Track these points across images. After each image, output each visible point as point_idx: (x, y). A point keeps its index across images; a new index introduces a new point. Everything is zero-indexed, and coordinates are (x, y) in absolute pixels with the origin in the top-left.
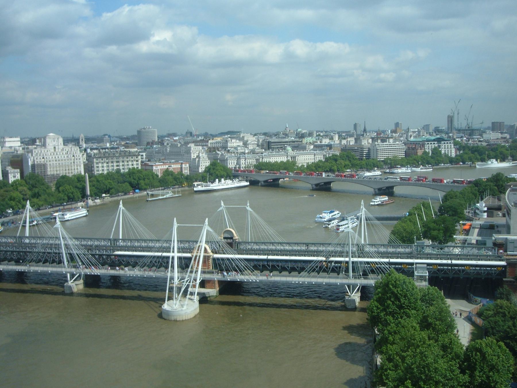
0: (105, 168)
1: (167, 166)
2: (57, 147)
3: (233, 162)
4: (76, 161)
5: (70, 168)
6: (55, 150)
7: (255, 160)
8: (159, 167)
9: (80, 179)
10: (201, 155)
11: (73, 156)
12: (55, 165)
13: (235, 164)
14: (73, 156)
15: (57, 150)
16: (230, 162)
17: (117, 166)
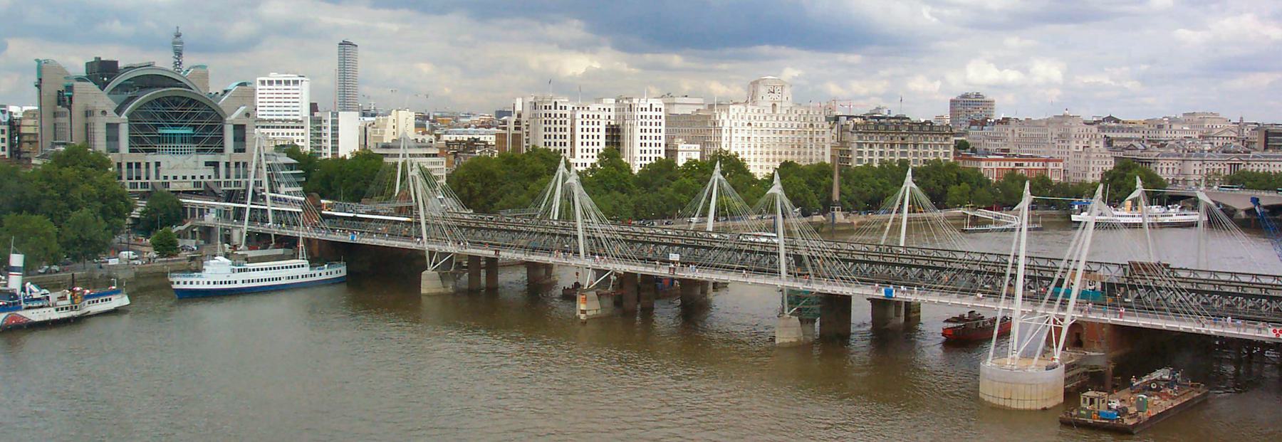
0: (876, 158)
1: (1013, 164)
2: (778, 105)
3: (1171, 166)
4: (815, 137)
5: (802, 150)
6: (774, 111)
7: (1228, 167)
8: (995, 165)
9: (822, 171)
10: (1093, 144)
11: (812, 125)
12: (772, 140)
13: (1176, 172)
14: (812, 125)
15: (778, 112)
16: (1165, 166)
17: (903, 153)
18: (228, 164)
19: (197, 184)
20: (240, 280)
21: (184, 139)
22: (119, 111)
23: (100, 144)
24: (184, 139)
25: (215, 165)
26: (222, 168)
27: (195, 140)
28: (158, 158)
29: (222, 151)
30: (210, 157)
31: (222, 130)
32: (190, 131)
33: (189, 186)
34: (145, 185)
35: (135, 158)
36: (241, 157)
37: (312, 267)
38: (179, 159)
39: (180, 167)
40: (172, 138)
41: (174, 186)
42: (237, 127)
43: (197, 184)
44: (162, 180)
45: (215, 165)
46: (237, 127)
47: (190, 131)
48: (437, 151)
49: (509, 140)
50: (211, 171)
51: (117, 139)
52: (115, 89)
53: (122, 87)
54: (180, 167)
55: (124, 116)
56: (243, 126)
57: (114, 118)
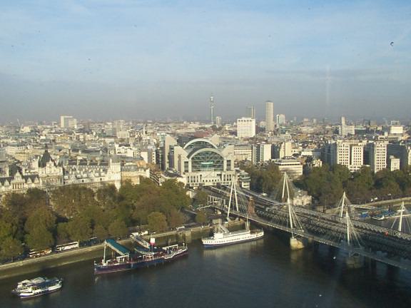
18: (225, 176)
19: (214, 183)
21: (210, 166)
22: (188, 157)
23: (183, 169)
24: (210, 166)
25: (220, 175)
26: (223, 177)
27: (214, 166)
28: (200, 173)
29: (222, 170)
31: (223, 162)
32: (212, 163)
34: (197, 184)
36: (229, 173)
37: (251, 233)
38: (208, 173)
40: (204, 166)
41: (206, 184)
42: (228, 161)
43: (214, 183)
44: (202, 182)
45: (220, 175)
46: (228, 161)
47: (212, 163)
48: (299, 163)
49: (326, 156)
50: (219, 178)
51: (188, 166)
53: (190, 146)
55: (190, 159)
56: (230, 161)
57: (187, 160)
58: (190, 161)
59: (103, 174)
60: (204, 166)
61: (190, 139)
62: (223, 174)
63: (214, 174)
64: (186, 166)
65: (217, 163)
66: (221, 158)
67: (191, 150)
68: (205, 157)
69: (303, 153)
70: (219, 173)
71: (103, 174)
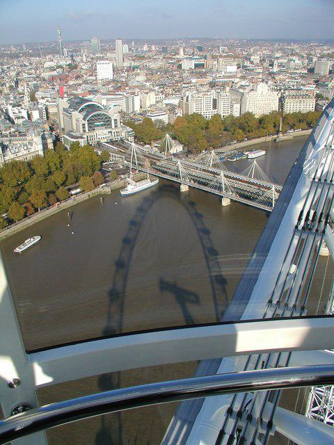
20: (137, 189)
21: (102, 125)
22: (84, 119)
24: (102, 125)
30: (110, 130)
33: (106, 141)
35: (91, 134)
39: (102, 134)
40: (98, 126)
52: (80, 112)
53: (83, 109)
54: (102, 134)
58: (86, 123)
59: (29, 146)
60: (98, 126)
61: (81, 104)
62: (113, 131)
63: (106, 131)
64: (84, 127)
65: (107, 122)
66: (110, 118)
67: (84, 113)
68: (95, 116)
69: (167, 101)
70: (110, 130)
71: (29, 146)
